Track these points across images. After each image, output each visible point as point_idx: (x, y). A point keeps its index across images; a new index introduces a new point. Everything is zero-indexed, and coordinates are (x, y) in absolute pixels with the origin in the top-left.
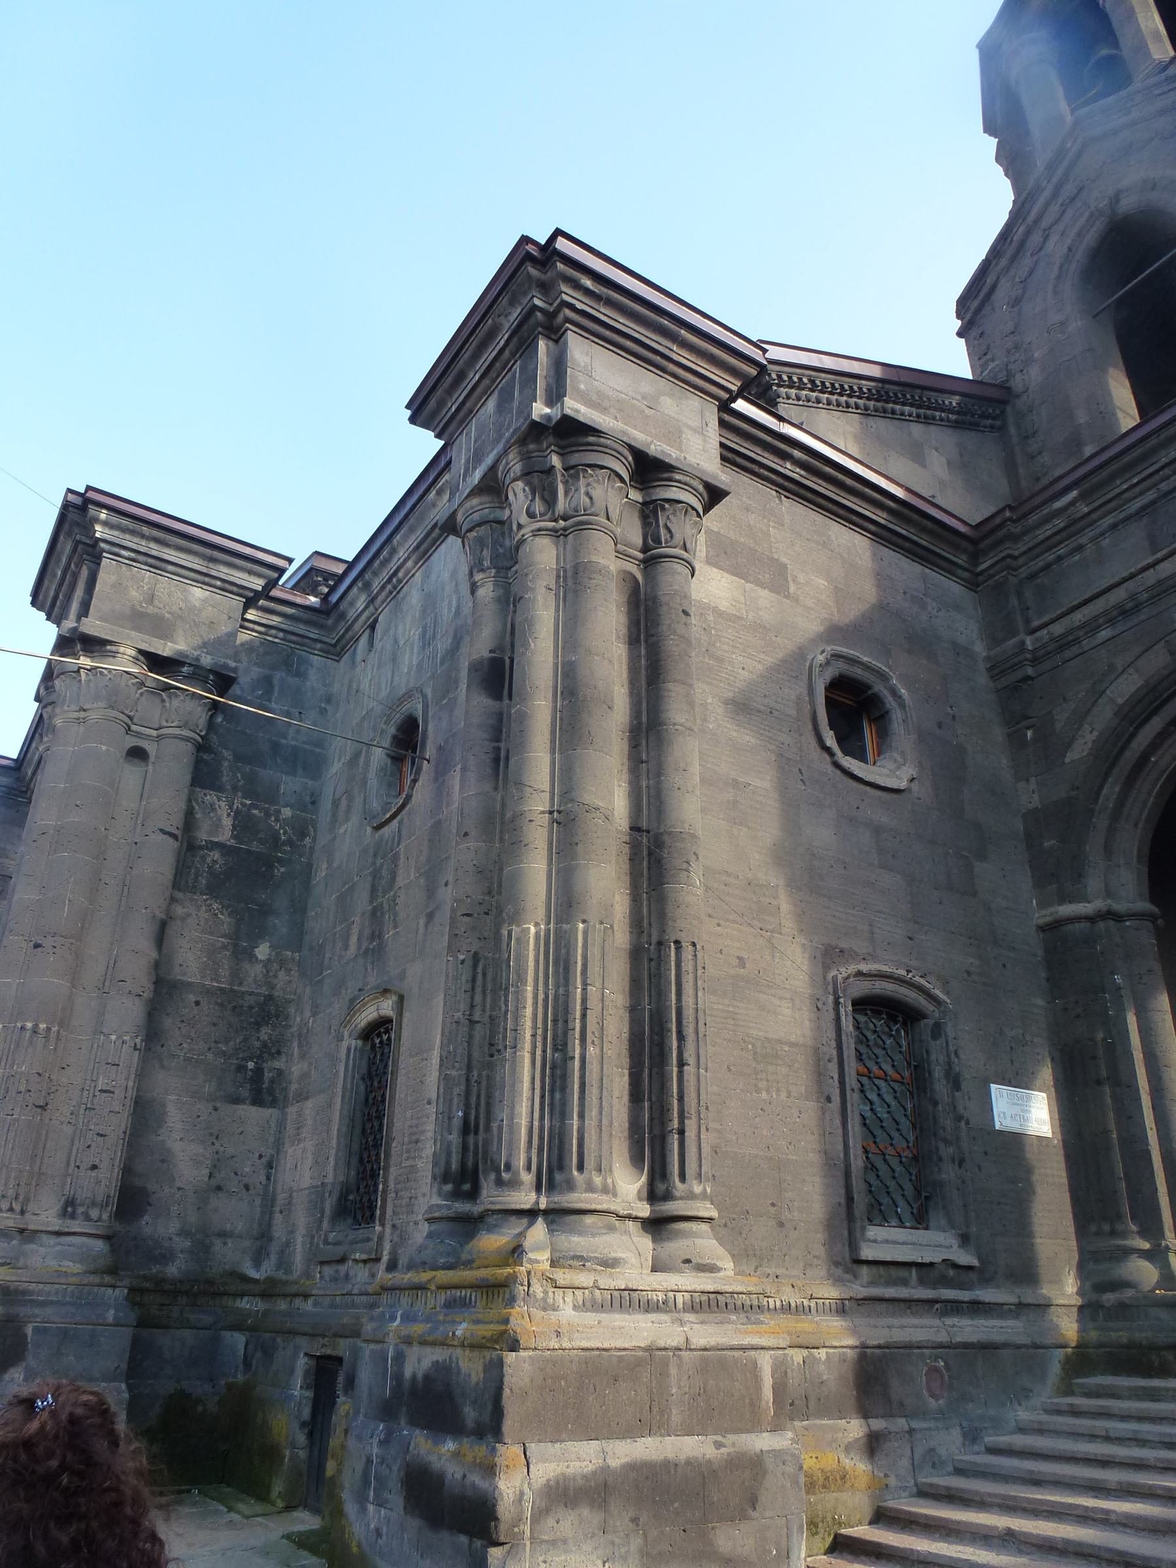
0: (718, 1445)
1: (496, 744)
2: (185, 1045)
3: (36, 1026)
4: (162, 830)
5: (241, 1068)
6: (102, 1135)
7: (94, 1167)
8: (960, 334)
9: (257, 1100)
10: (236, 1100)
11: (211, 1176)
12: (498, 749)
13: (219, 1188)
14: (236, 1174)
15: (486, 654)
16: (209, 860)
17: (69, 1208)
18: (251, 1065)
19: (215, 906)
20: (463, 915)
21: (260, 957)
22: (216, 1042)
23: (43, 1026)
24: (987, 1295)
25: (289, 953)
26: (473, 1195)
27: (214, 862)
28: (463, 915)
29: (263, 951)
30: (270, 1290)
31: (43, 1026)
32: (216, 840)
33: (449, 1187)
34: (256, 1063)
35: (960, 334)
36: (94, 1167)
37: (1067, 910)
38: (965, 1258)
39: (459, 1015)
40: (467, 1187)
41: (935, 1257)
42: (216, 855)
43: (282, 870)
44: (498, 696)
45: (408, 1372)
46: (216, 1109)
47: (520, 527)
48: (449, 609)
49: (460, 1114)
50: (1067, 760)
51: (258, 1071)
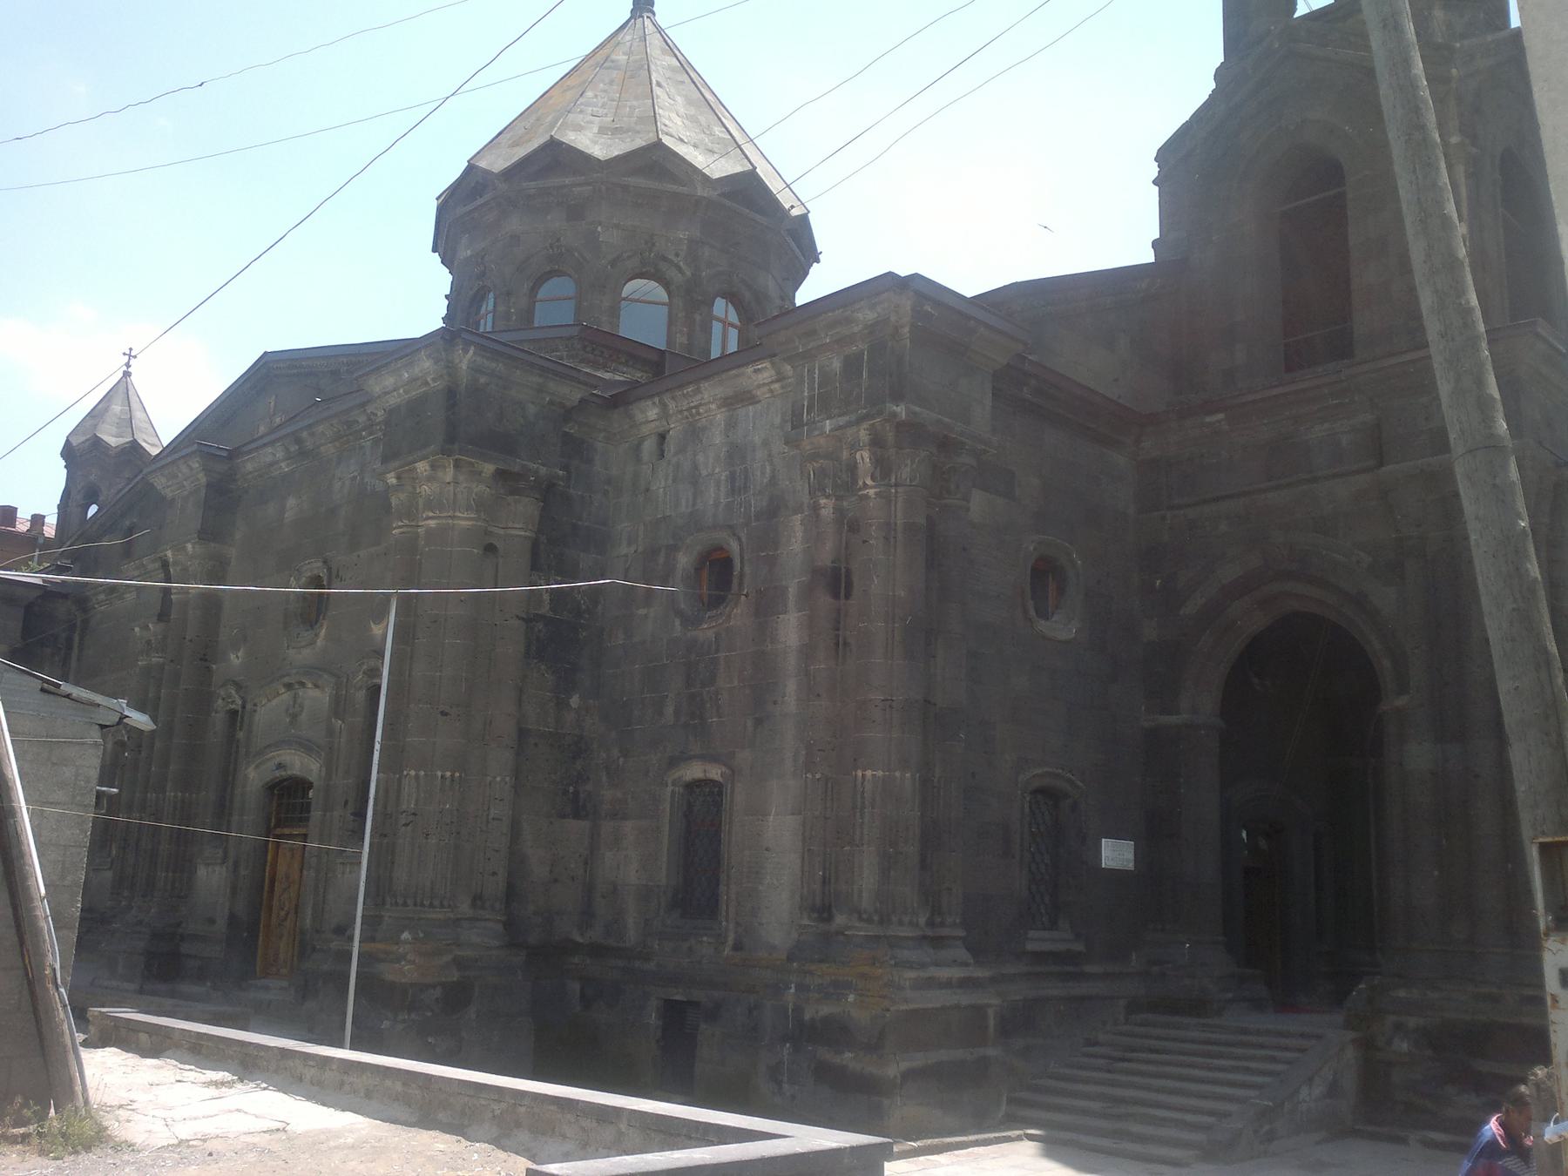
0: (972, 1054)
1: (837, 632)
2: (530, 778)
3: (452, 776)
4: (517, 616)
5: (565, 792)
6: (497, 851)
7: (494, 874)
8: (1155, 182)
9: (577, 815)
10: (563, 816)
11: (551, 871)
12: (838, 636)
13: (556, 881)
14: (566, 869)
15: (829, 564)
16: (536, 629)
17: (477, 900)
18: (571, 789)
19: (543, 667)
20: (819, 750)
21: (573, 706)
22: (549, 773)
23: (457, 774)
24: (1089, 969)
25: (591, 701)
26: (830, 919)
27: (540, 631)
28: (819, 750)
29: (575, 701)
30: (597, 951)
31: (457, 774)
32: (540, 612)
33: (816, 915)
34: (575, 787)
35: (1155, 182)
36: (494, 874)
37: (1165, 720)
38: (1079, 947)
39: (817, 813)
40: (825, 915)
41: (1061, 947)
42: (540, 626)
43: (584, 634)
44: (836, 596)
45: (807, 1017)
46: (551, 823)
47: (865, 486)
48: (763, 473)
49: (821, 873)
50: (1181, 613)
51: (576, 793)
